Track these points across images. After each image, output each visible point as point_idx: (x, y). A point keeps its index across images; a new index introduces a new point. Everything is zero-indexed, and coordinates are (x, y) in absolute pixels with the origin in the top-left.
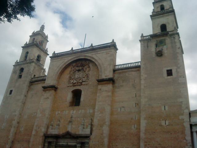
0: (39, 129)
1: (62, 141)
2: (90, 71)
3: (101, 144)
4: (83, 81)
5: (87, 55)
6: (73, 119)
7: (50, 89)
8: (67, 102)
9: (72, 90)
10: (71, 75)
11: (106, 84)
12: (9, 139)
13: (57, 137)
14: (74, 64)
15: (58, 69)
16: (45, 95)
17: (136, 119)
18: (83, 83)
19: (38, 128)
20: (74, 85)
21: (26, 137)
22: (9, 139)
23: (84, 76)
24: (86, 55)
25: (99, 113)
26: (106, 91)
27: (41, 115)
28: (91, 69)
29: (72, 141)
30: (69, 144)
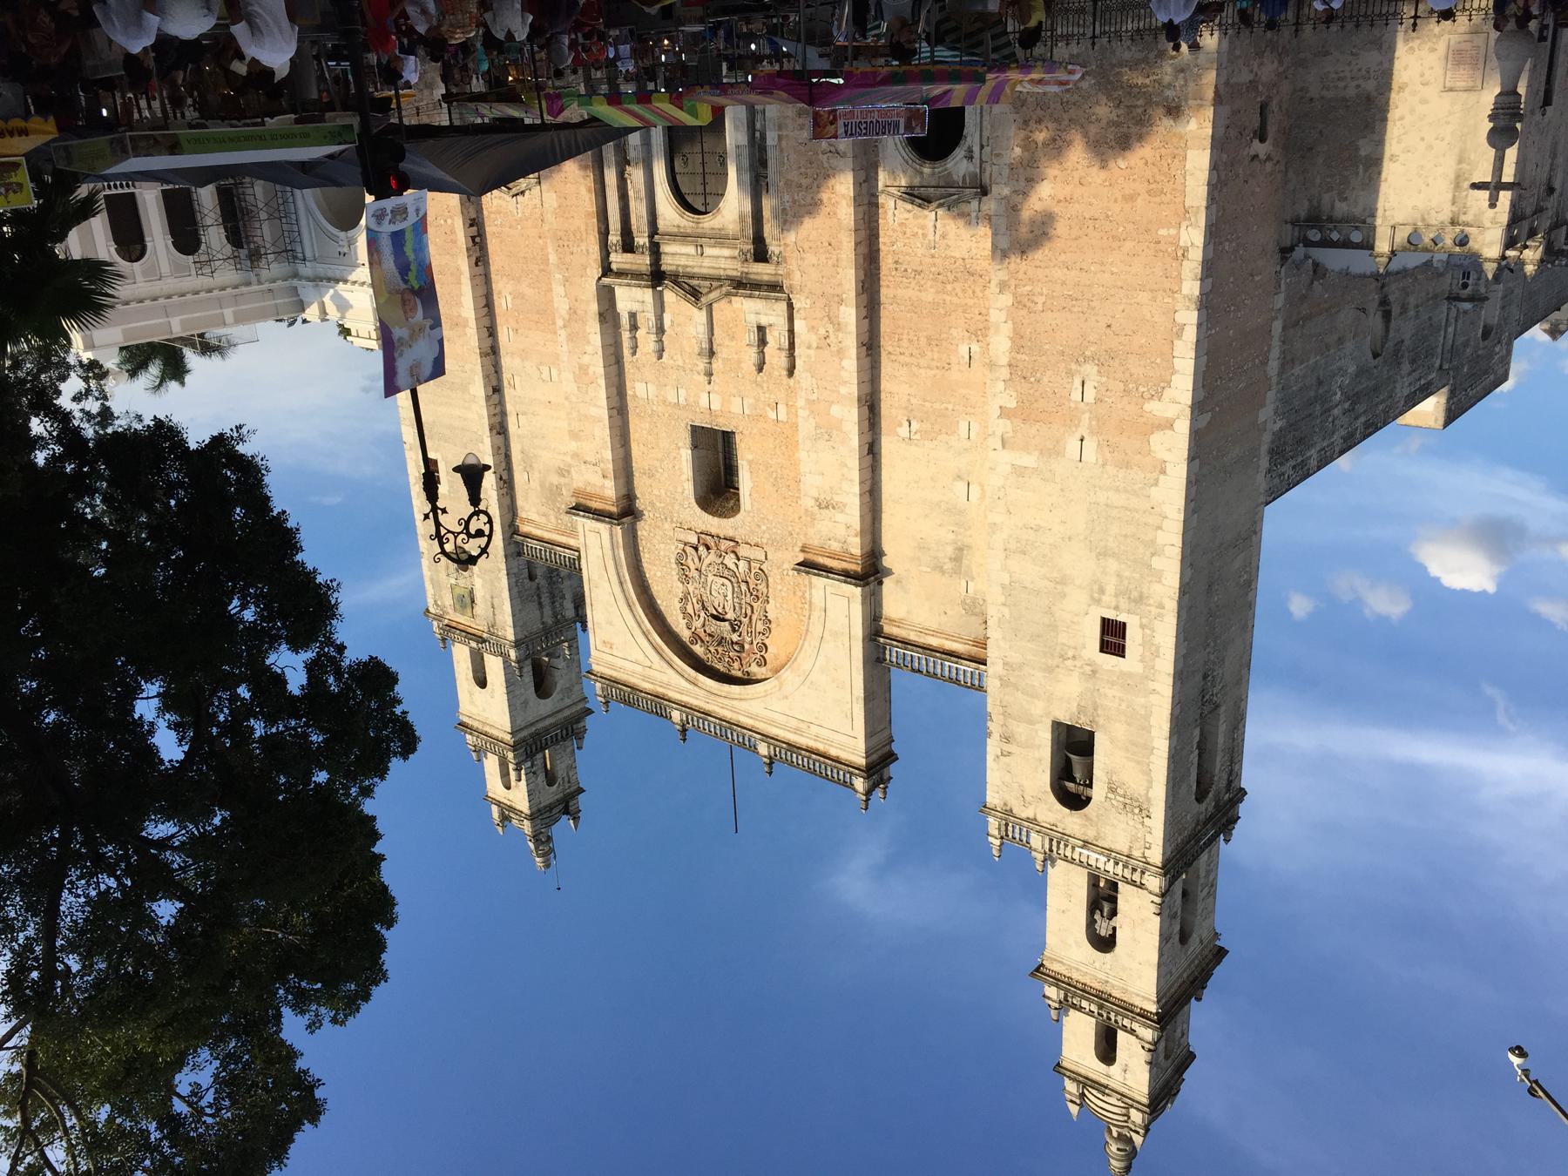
0: (822, 332)
1: (723, 264)
3: (561, 243)
5: (685, 684)
6: (701, 365)
7: (821, 560)
9: (739, 516)
11: (591, 496)
12: (1003, 286)
13: (742, 285)
14: (754, 669)
16: (841, 531)
18: (694, 540)
19: (832, 339)
21: (928, 296)
22: (1003, 286)
23: (695, 574)
24: (690, 687)
25: (591, 371)
27: (836, 410)
29: (683, 261)
30: (691, 250)
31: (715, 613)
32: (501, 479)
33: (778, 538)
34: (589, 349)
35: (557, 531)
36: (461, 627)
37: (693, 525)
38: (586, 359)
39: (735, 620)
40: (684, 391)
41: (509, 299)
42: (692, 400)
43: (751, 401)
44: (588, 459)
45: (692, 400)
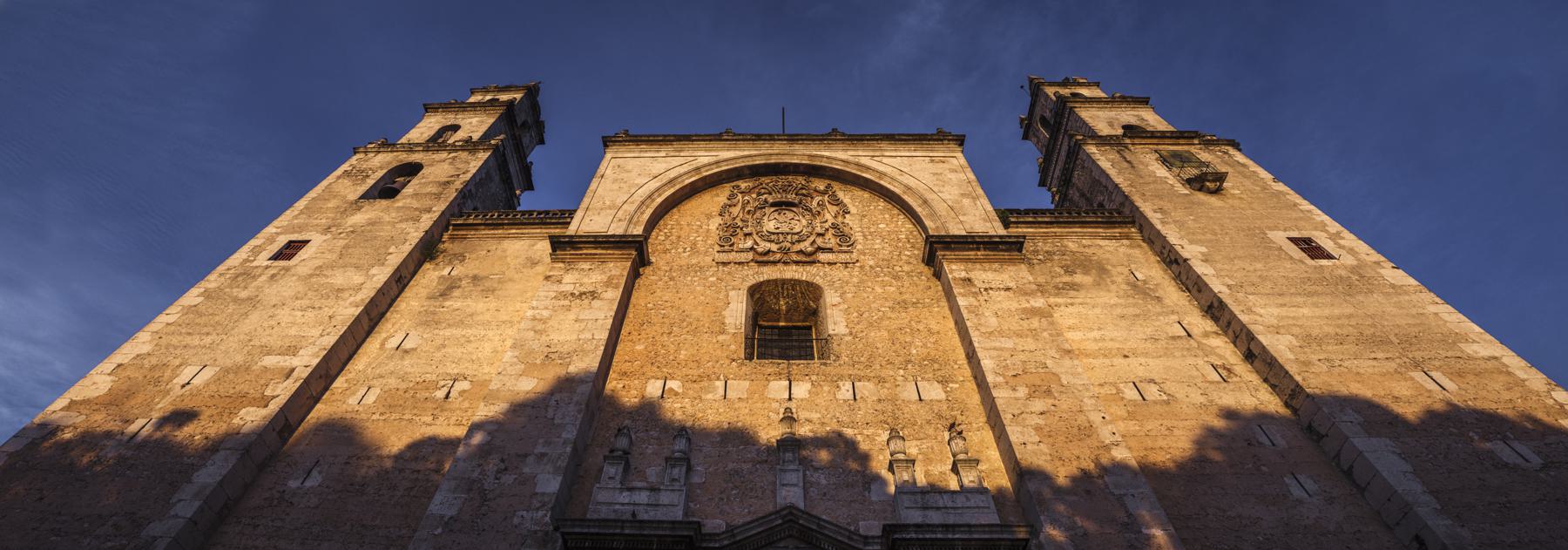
2: (847, 216)
4: (822, 245)
8: (723, 332)
10: (734, 219)
15: (654, 184)
17: (1280, 442)
18: (822, 257)
20: (763, 259)
25: (1022, 392)
26: (1008, 289)
28: (853, 210)
31: (794, 209)
32: (1176, 261)
33: (692, 274)
34: (1040, 421)
35: (1055, 235)
36: (1167, 141)
37: (827, 269)
38: (1038, 405)
39: (764, 208)
40: (839, 396)
41: (1296, 492)
42: (826, 388)
43: (710, 396)
44: (1002, 292)
45: (826, 388)
